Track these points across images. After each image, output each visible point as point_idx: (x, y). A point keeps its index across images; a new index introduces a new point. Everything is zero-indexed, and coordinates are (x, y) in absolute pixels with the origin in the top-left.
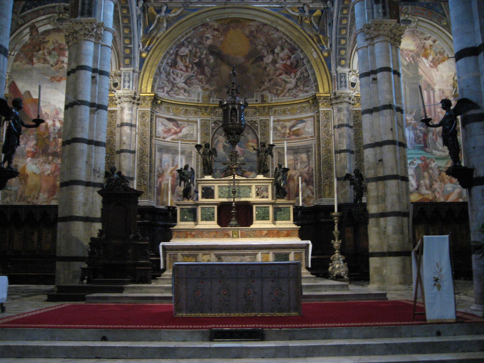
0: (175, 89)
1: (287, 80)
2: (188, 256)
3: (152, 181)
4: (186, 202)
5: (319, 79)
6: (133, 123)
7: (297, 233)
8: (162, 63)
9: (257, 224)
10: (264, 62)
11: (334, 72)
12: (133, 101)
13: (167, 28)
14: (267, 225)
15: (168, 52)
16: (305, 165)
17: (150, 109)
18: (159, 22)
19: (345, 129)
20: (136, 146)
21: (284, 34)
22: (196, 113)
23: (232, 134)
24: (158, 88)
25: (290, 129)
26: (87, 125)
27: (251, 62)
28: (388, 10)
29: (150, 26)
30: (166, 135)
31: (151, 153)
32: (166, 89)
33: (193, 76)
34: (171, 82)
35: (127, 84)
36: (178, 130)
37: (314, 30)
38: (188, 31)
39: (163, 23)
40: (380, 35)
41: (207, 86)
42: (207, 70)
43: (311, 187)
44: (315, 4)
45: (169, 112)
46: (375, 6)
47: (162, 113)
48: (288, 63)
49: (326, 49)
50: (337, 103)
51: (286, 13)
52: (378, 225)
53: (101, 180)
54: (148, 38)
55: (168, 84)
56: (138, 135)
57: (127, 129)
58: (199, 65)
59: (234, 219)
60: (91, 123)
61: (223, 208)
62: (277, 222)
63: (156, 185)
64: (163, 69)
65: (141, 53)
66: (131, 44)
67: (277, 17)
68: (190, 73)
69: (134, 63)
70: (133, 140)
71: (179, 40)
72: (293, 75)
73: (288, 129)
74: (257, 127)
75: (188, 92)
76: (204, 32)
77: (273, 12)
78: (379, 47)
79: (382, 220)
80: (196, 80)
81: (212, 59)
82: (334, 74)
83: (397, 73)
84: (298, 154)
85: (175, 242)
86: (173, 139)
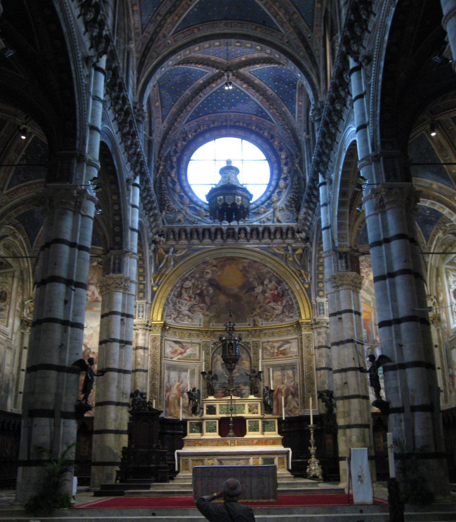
0: (181, 316)
1: (275, 307)
2: (197, 461)
3: (162, 395)
4: (194, 417)
5: (301, 307)
6: (146, 346)
7: (280, 442)
8: (170, 295)
9: (250, 435)
10: (255, 292)
11: (314, 301)
12: (146, 328)
13: (174, 266)
14: (257, 435)
15: (175, 286)
16: (291, 380)
17: (160, 335)
18: (167, 261)
19: (324, 350)
20: (148, 366)
21: (272, 269)
22: (198, 336)
23: (229, 363)
24: (167, 316)
25: (278, 349)
26: (117, 357)
27: (244, 292)
28: (349, 264)
29: (160, 263)
30: (172, 356)
31: (161, 372)
32: (173, 316)
33: (195, 305)
34: (178, 310)
35: (141, 314)
36: (183, 351)
37: (297, 266)
38: (191, 268)
39: (170, 262)
40: (343, 284)
41: (207, 313)
42: (207, 299)
43: (296, 399)
44: (297, 244)
45: (175, 335)
46: (339, 261)
47: (170, 337)
48: (276, 293)
49: (307, 281)
50: (317, 328)
51: (273, 252)
52: (345, 434)
53: (127, 400)
54: (158, 274)
55: (174, 312)
56: (151, 356)
57: (141, 352)
58: (201, 295)
59: (231, 431)
60: (121, 356)
61: (222, 421)
62: (266, 433)
63: (165, 399)
64: (171, 299)
65: (152, 287)
66: (144, 280)
67: (265, 255)
68: (193, 302)
69: (147, 296)
70: (146, 361)
71: (183, 276)
72: (279, 303)
73: (276, 348)
74: (250, 348)
75: (191, 318)
76: (204, 269)
77: (263, 251)
78: (343, 293)
79: (348, 430)
80: (198, 308)
81: (211, 290)
82: (314, 303)
83: (358, 313)
84: (285, 371)
85: (186, 450)
86: (179, 359)
